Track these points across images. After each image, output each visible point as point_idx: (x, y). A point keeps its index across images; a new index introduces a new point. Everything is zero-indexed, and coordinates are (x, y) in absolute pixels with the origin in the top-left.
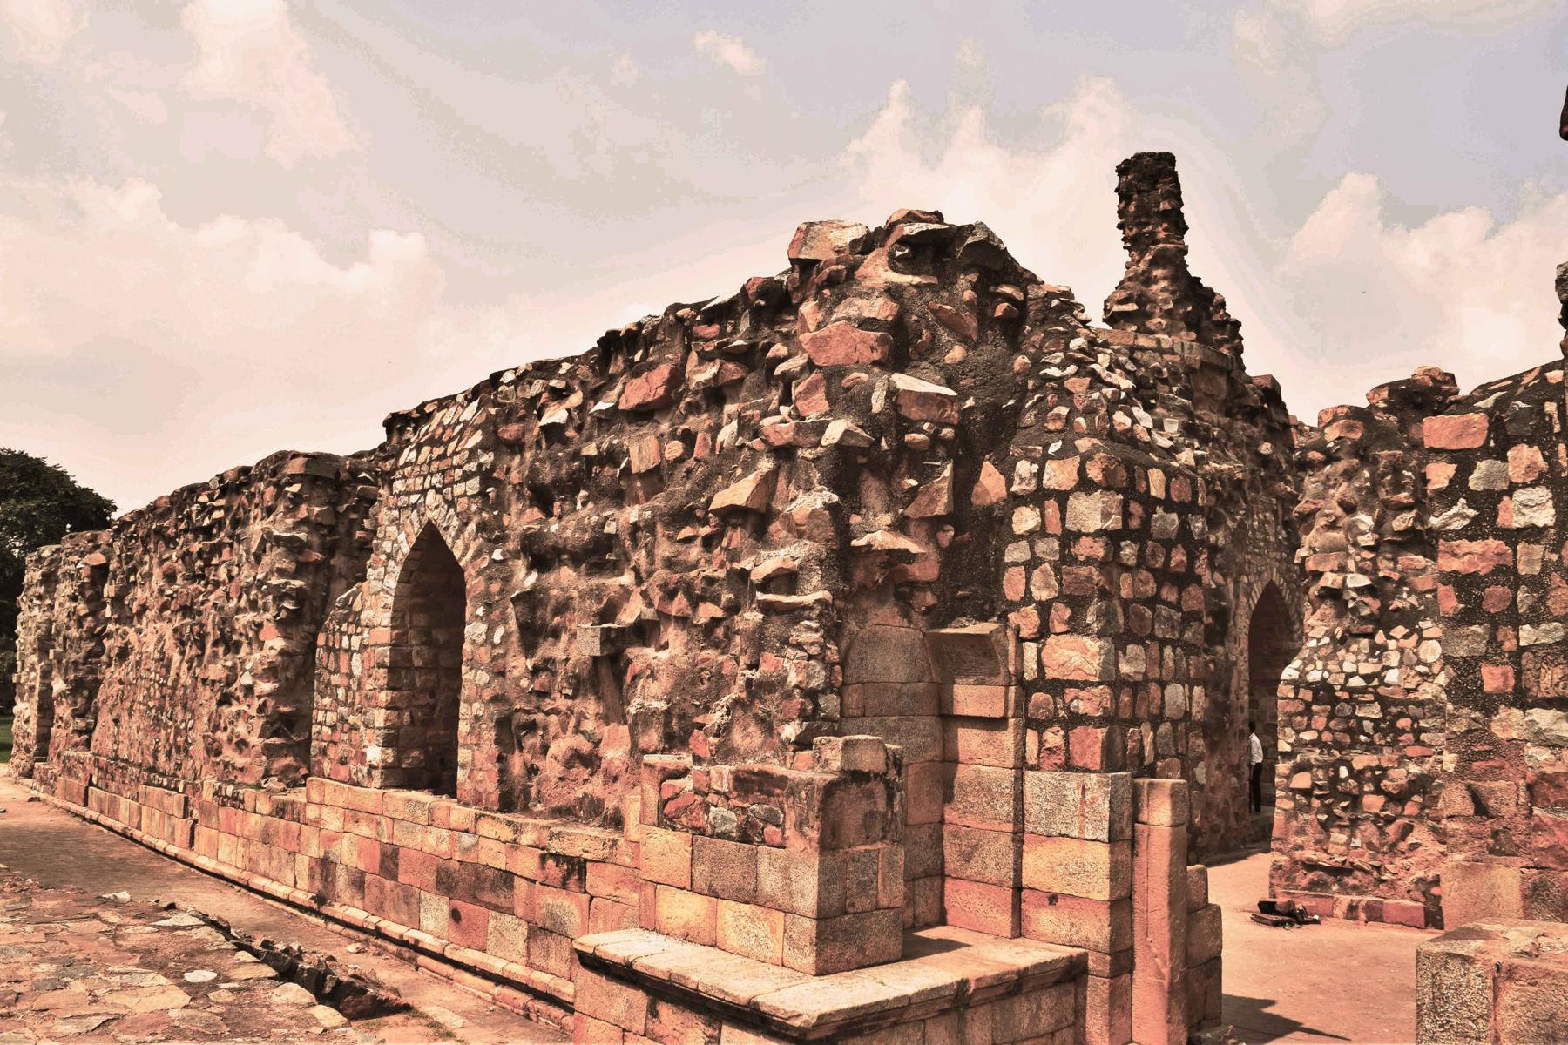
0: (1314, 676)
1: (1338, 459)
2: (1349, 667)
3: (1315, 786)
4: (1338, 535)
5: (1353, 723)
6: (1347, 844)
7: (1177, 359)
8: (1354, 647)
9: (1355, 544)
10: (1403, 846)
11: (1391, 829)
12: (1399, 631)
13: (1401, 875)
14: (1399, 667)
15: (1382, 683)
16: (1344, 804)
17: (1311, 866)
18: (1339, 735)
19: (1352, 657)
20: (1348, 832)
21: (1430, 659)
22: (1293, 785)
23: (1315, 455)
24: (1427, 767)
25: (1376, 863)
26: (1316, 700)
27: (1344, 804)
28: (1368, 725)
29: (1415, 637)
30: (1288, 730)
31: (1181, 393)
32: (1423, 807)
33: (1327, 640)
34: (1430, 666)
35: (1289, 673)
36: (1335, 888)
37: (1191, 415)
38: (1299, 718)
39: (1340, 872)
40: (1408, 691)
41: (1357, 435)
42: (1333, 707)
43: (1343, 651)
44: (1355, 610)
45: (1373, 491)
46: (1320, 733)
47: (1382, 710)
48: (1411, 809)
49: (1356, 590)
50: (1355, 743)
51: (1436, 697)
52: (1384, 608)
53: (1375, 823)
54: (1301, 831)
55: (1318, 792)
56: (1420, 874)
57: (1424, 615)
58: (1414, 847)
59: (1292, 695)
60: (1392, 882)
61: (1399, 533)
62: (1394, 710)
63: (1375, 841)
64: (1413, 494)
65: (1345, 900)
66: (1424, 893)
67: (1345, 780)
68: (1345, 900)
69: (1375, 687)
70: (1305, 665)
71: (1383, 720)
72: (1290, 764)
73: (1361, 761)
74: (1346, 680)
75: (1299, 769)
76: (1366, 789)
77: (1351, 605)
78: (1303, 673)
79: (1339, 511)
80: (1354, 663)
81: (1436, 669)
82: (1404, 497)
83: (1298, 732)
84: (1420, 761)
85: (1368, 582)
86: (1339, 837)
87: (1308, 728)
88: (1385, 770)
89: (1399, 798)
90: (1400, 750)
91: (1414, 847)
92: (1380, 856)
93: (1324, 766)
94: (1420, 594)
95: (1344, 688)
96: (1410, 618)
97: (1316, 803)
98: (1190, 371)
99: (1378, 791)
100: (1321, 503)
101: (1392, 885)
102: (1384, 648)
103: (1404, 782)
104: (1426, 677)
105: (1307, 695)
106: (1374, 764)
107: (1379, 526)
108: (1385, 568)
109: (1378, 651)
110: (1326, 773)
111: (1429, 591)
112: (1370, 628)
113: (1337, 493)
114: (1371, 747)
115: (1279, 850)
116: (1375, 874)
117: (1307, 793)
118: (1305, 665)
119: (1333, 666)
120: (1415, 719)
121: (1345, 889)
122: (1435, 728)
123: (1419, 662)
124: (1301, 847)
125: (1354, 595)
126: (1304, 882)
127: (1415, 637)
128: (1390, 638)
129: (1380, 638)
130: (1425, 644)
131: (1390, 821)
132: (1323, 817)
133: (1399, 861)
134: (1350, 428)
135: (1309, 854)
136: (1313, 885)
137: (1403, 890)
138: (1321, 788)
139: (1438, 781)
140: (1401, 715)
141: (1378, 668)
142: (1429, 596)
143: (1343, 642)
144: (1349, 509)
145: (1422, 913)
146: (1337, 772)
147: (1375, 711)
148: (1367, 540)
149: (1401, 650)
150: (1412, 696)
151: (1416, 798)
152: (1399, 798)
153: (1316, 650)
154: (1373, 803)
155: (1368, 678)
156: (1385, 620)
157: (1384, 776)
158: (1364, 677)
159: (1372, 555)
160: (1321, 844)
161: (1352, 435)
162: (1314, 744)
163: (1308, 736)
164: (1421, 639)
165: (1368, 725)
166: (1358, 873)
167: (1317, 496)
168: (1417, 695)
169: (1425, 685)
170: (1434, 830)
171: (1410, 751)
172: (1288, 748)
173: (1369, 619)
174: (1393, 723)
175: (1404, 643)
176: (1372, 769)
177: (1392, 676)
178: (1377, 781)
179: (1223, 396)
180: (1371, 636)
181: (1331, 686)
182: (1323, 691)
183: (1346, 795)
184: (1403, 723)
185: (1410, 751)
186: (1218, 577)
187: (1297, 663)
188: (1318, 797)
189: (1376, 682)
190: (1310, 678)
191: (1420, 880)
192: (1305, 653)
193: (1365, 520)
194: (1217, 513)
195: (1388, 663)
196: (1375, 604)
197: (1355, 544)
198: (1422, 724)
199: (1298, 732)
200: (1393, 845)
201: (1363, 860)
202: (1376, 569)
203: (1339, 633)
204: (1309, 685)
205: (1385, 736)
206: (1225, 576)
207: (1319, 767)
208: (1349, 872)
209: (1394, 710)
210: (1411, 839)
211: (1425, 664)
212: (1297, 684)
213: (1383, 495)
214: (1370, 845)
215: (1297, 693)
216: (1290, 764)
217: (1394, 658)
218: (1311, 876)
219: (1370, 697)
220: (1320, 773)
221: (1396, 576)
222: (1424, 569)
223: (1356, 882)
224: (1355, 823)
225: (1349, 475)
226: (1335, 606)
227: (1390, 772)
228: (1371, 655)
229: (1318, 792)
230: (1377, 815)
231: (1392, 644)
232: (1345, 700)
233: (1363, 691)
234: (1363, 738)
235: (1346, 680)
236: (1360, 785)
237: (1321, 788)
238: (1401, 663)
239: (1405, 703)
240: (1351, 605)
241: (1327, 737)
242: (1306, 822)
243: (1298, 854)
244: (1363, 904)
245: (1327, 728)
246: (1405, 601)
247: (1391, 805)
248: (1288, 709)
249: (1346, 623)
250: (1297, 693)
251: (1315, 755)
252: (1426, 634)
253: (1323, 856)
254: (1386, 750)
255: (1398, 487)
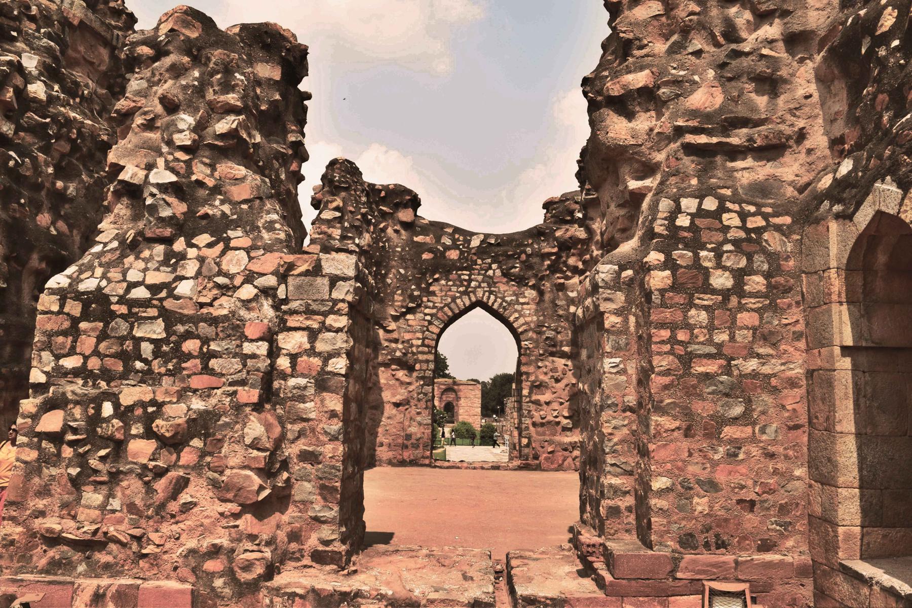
0: (89, 284)
1: (167, 53)
2: (134, 276)
3: (66, 428)
4: (154, 136)
5: (129, 345)
6: (102, 507)
7: (54, 7)
8: (146, 253)
9: (170, 143)
10: (173, 507)
11: (161, 485)
12: (203, 239)
13: (168, 546)
14: (195, 278)
15: (171, 295)
16: (103, 452)
17: (53, 540)
18: (109, 362)
19: (141, 265)
20: (104, 490)
21: (233, 270)
22: (39, 429)
23: (145, 50)
24: (213, 401)
25: (137, 532)
26: (86, 315)
27: (103, 452)
28: (147, 349)
29: (221, 246)
30: (46, 355)
31: (49, 36)
32: (203, 454)
33: (115, 244)
34: (231, 277)
35: (59, 281)
36: (81, 568)
37: (55, 59)
38: (61, 339)
39: (89, 545)
40: (202, 305)
41: (194, 35)
42: (107, 324)
43: (131, 258)
44: (153, 209)
45: (200, 91)
46: (86, 358)
47: (166, 329)
48: (188, 456)
49: (159, 186)
50: (128, 371)
51: (233, 313)
52: (190, 213)
53: (140, 476)
54: (44, 492)
55: (70, 437)
56: (192, 544)
57: (235, 225)
58: (187, 507)
59: (55, 308)
60: (156, 556)
61: (222, 136)
62: (180, 328)
63: (138, 502)
64: (243, 98)
65: (90, 585)
66: (194, 570)
67: (107, 420)
68: (90, 585)
69: (161, 300)
70: (81, 272)
71: (166, 341)
72: (39, 400)
73: (130, 394)
74: (128, 290)
75: (49, 406)
76: (134, 431)
77: (149, 201)
78: (75, 280)
79: (159, 109)
80: (144, 271)
81: (238, 281)
82: (232, 98)
83: (57, 357)
84: (206, 393)
85: (173, 178)
86: (92, 497)
87: (72, 352)
88: (160, 405)
89: (174, 443)
90: (183, 380)
91: (187, 507)
92: (143, 523)
93: (83, 401)
94: (235, 204)
95: (122, 300)
96: (218, 228)
97: (68, 452)
98: (65, 22)
99: (149, 434)
100: (143, 101)
101: (154, 560)
102: (182, 256)
103: (180, 421)
104: (225, 290)
105: (74, 308)
106: (147, 398)
107: (199, 128)
108: (200, 172)
109: (173, 260)
110: (86, 411)
111: (245, 201)
112: (168, 232)
113: (160, 90)
114: (148, 377)
115: (12, 519)
116: (135, 547)
117: (56, 438)
118: (81, 272)
119: (115, 274)
120: (206, 341)
121: (95, 570)
122: (228, 352)
123: (220, 273)
124: (42, 514)
125: (155, 191)
126: (43, 562)
127: (221, 246)
128: (190, 245)
129: (179, 245)
130: (230, 254)
131: (160, 473)
132: (74, 471)
133: (167, 528)
134: (187, 24)
135: (52, 523)
136: (54, 566)
137: (168, 567)
138: (75, 431)
139: (225, 419)
140: (188, 335)
141: (169, 278)
142: (245, 207)
143: (131, 247)
144: (171, 107)
145: (189, 598)
146: (98, 409)
147: (157, 330)
148: (184, 139)
149: (202, 260)
150: (204, 311)
151: (196, 443)
152: (174, 443)
153: (99, 255)
154: (141, 449)
155: (154, 289)
156: (186, 227)
157: (158, 414)
158: (149, 287)
159: (187, 157)
160: (69, 509)
161: (188, 32)
162: (76, 372)
163: (70, 363)
164: (227, 248)
165: (147, 349)
166: (113, 547)
167: (138, 93)
168: (211, 310)
169: (224, 300)
170: (215, 484)
171: (197, 382)
172: (42, 379)
173: (171, 221)
174: (178, 345)
175: (207, 252)
176: (143, 405)
177: (184, 288)
178: (148, 420)
179: (103, 68)
180: (168, 241)
181: (107, 297)
182: (96, 305)
183: (109, 440)
184: (191, 346)
185: (197, 382)
186: (61, 224)
187: (72, 270)
188: (71, 444)
189: (163, 294)
190: (82, 287)
191: (193, 552)
192: (86, 259)
193: (186, 120)
194: (70, 163)
195: (183, 273)
196: (180, 208)
197: (170, 143)
198: (213, 346)
199: (57, 357)
200: (162, 506)
201: (120, 529)
202: (190, 172)
203: (130, 235)
204: (78, 296)
205: (166, 363)
206: (71, 227)
207: (77, 403)
208: (101, 546)
209: (180, 328)
210: (184, 497)
211: (226, 275)
212: (63, 295)
213: (210, 95)
214: (131, 507)
215: (62, 306)
216: (39, 400)
217: (191, 268)
218: (53, 553)
219: (152, 312)
220: (77, 412)
221: (210, 182)
222: (243, 179)
223: (108, 559)
224: (115, 477)
225: (177, 71)
226: (132, 206)
227: (168, 410)
228: (165, 262)
229: (70, 437)
230: (144, 467)
231: (192, 253)
232: (122, 316)
233: (145, 304)
234: (139, 365)
235: (128, 290)
236: (127, 427)
237: (75, 431)
238: (199, 273)
239: (195, 320)
240: (149, 201)
241: (94, 364)
242: (52, 478)
243: (39, 524)
244: (113, 589)
245: (96, 353)
246: (217, 208)
247: (164, 452)
248: (48, 327)
249: (141, 225)
250: (62, 306)
251: (75, 388)
252: (233, 244)
253: (70, 524)
254: (166, 381)
255: (227, 87)
